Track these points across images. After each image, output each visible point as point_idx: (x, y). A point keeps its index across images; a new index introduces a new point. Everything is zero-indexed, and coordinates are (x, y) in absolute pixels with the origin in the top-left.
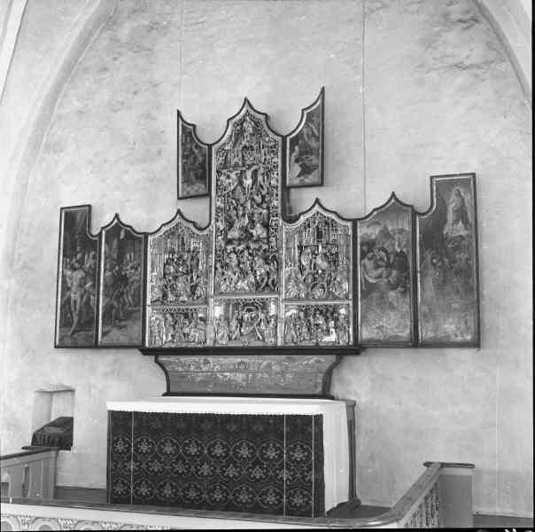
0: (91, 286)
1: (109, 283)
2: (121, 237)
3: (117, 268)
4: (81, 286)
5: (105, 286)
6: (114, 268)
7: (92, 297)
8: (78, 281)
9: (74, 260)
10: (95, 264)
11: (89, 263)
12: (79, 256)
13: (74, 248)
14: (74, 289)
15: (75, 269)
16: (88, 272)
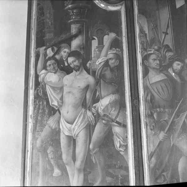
0: (113, 104)
1: (161, 96)
2: (178, 6)
3: (177, 65)
4: (87, 101)
5: (152, 103)
6: (170, 65)
7: (117, 130)
8: (78, 94)
9: (64, 52)
10: (119, 58)
11: (100, 58)
12: (75, 43)
13: (62, 27)
14: (67, 111)
15: (67, 70)
16: (102, 76)
